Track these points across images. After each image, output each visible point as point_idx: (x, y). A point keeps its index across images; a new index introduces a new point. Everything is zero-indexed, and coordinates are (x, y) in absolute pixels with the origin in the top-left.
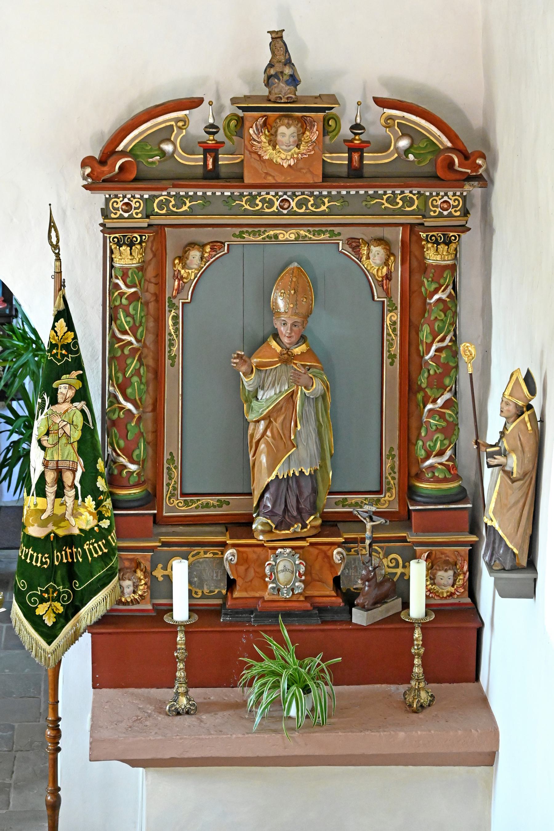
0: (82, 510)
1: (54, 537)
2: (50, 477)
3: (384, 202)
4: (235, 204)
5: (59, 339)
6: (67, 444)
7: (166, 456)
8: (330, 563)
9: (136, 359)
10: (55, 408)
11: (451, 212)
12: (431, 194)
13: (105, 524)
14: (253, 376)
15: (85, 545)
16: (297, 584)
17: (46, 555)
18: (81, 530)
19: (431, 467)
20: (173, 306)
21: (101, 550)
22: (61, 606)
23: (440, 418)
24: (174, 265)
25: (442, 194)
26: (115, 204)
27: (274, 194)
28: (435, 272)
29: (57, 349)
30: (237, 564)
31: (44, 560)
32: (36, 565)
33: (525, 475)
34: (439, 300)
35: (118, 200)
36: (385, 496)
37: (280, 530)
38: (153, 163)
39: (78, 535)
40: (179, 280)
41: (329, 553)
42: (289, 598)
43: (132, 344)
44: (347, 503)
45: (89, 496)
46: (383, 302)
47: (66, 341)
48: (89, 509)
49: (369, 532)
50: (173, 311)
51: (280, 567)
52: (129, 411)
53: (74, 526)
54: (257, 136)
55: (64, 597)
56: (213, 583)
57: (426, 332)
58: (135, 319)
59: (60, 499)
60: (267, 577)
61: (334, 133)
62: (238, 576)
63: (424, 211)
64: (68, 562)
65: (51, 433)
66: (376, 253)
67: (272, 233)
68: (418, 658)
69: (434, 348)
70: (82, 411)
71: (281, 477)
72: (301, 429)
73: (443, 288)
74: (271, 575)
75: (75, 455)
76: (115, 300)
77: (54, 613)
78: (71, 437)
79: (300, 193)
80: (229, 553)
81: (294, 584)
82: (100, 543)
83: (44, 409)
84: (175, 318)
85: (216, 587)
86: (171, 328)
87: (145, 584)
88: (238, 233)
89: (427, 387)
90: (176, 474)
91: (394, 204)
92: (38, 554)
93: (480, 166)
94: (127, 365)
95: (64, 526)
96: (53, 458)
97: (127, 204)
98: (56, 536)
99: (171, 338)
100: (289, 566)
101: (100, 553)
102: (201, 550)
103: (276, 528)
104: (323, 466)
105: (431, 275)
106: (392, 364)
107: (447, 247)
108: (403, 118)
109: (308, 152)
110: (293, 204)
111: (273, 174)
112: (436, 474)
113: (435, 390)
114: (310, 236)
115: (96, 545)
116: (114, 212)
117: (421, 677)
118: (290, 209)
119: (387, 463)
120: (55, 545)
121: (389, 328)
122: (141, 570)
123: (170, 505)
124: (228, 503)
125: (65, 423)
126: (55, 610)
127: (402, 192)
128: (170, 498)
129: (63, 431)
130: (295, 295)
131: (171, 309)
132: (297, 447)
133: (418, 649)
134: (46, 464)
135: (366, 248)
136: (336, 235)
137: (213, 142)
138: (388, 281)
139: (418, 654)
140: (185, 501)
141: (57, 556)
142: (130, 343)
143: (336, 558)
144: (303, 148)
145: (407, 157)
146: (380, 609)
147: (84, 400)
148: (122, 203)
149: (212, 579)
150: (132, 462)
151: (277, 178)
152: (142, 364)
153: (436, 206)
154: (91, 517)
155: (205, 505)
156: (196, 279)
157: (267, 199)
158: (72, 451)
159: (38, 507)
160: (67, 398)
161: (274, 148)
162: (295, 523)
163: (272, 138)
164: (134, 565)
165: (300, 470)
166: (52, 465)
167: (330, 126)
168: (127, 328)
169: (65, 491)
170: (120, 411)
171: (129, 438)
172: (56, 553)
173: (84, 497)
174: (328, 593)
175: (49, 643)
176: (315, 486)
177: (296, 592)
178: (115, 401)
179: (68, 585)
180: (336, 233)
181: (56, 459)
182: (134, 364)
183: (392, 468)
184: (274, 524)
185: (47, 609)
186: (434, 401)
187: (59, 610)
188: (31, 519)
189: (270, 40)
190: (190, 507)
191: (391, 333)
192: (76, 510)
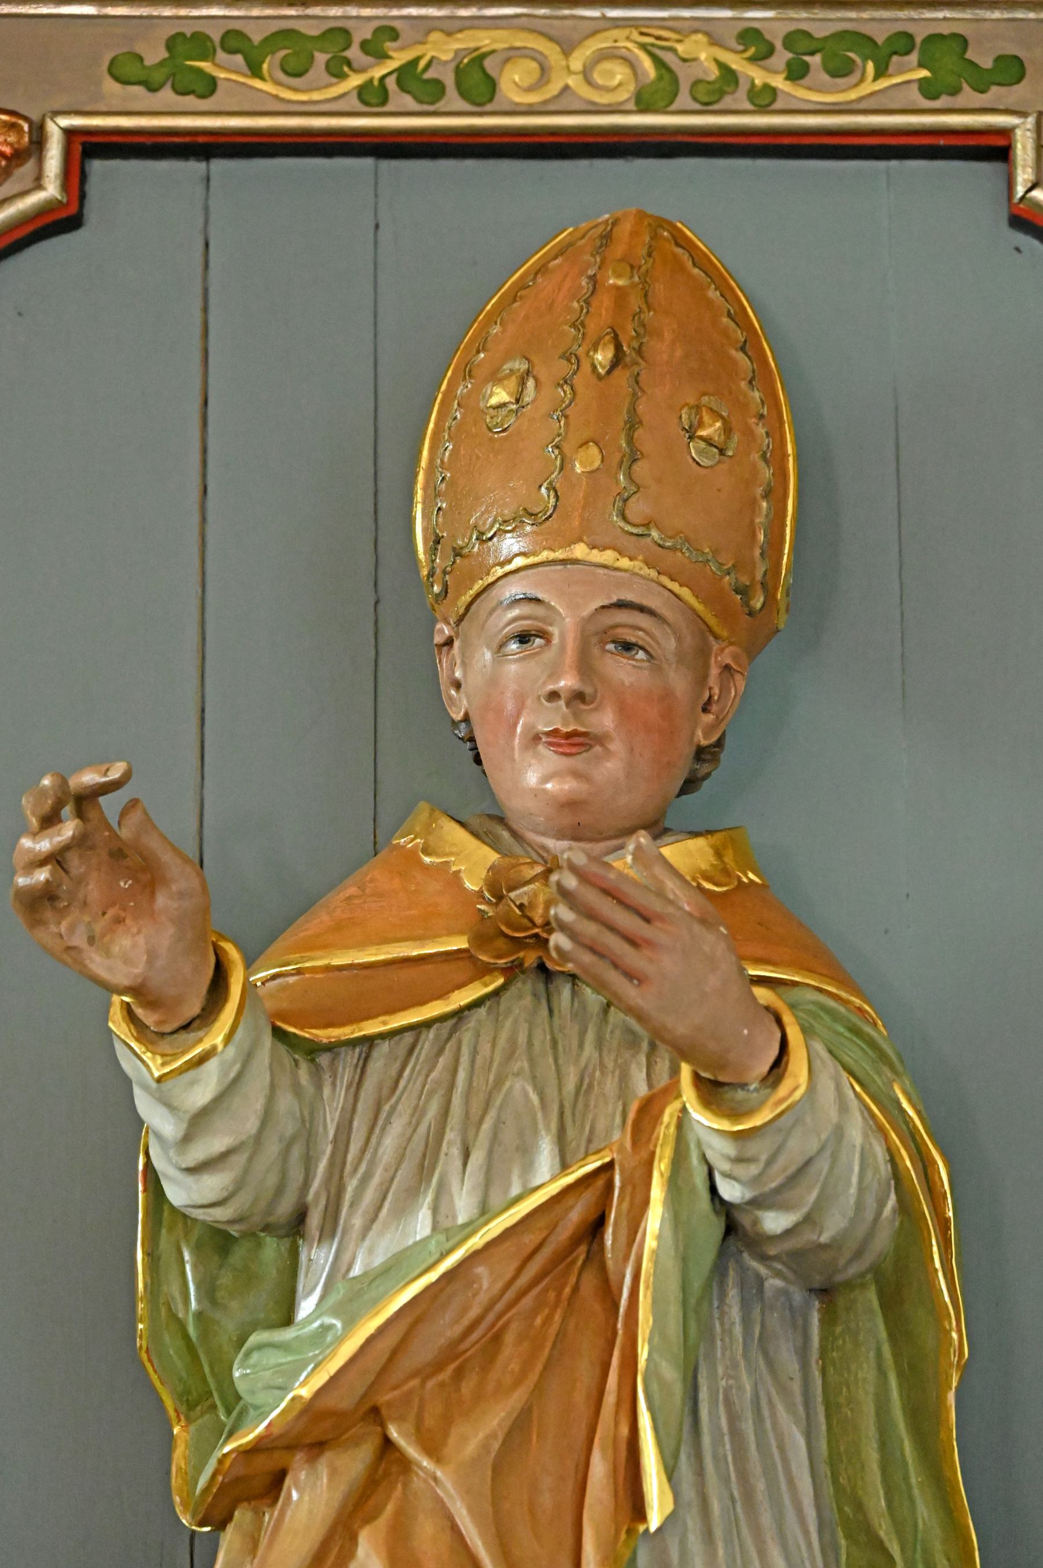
14: (216, 1036)
72: (670, 1520)
114: (759, 76)
130: (622, 377)
136: (982, 82)
180: (987, 63)
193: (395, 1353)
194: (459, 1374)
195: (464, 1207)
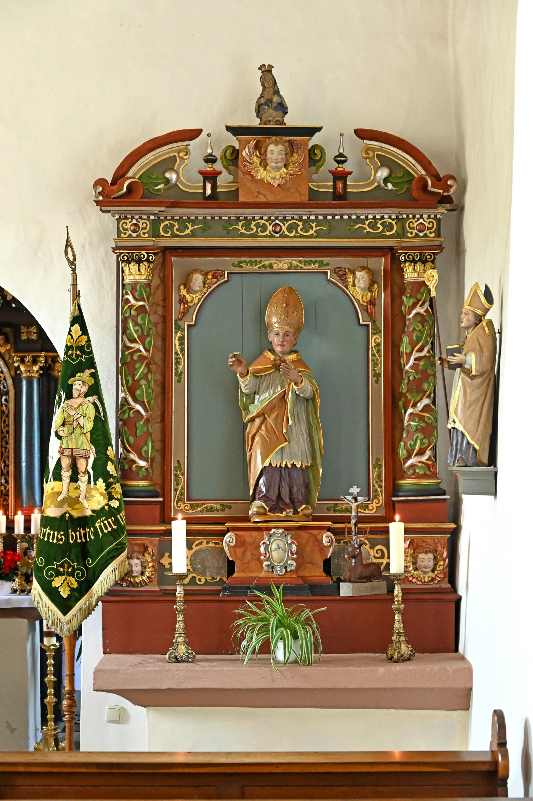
0: (94, 493)
1: (69, 517)
2: (66, 463)
3: (366, 226)
4: (232, 228)
5: (75, 341)
6: (81, 434)
8: (320, 546)
9: (144, 364)
10: (70, 402)
11: (426, 233)
12: (408, 216)
13: (115, 504)
14: (248, 377)
15: (97, 523)
16: (289, 562)
17: (62, 533)
18: (93, 511)
19: (412, 466)
20: (178, 328)
21: (111, 526)
23: (420, 419)
24: (179, 290)
25: (418, 216)
26: (124, 225)
27: (267, 219)
28: (413, 288)
29: (73, 350)
30: (234, 547)
31: (59, 537)
32: (53, 542)
33: (482, 374)
34: (417, 314)
36: (372, 503)
37: (274, 513)
38: (159, 190)
39: (91, 516)
40: (184, 304)
41: (319, 537)
42: (282, 575)
43: (141, 351)
44: (338, 508)
45: (100, 478)
46: (368, 325)
47: (81, 343)
48: (100, 490)
49: (355, 512)
50: (179, 332)
51: (274, 546)
52: (138, 411)
54: (250, 158)
55: (78, 574)
56: (215, 570)
57: (406, 343)
58: (143, 328)
59: (74, 483)
60: (261, 555)
61: (320, 163)
62: (237, 558)
63: (402, 235)
64: (82, 542)
65: (67, 424)
66: (361, 277)
67: (267, 263)
68: (398, 613)
69: (412, 358)
70: (95, 404)
71: (274, 465)
73: (420, 303)
74: (266, 553)
75: (88, 443)
76: (126, 312)
77: (69, 586)
79: (290, 218)
80: (229, 537)
81: (287, 562)
82: (110, 520)
83: (60, 403)
85: (218, 574)
86: (177, 347)
87: (153, 567)
88: (236, 263)
89: (407, 392)
90: (184, 480)
91: (376, 228)
92: (54, 532)
93: (451, 186)
94: (136, 369)
95: (78, 508)
96: (69, 447)
97: (135, 225)
98: (71, 516)
99: (178, 357)
100: (281, 544)
101: (110, 529)
102: (204, 540)
103: (269, 511)
104: (314, 466)
105: (410, 291)
106: (377, 382)
107: (423, 265)
108: (381, 149)
109: (295, 172)
110: (284, 228)
111: (264, 193)
112: (417, 471)
113: (415, 394)
114: (301, 265)
115: (106, 522)
116: (124, 232)
117: (401, 631)
118: (281, 233)
119: (373, 472)
120: (69, 525)
121: (374, 349)
122: (149, 554)
123: (179, 509)
125: (79, 416)
126: (70, 585)
127: (382, 218)
128: (177, 504)
129: (78, 423)
131: (177, 331)
132: (289, 443)
133: (398, 604)
134: (62, 452)
135: (352, 277)
136: (325, 265)
137: (211, 169)
138: (372, 306)
139: (399, 610)
140: (191, 504)
141: (72, 535)
142: (139, 351)
143: (325, 540)
144: (291, 168)
145: (386, 186)
146: (366, 585)
147: (96, 395)
148: (131, 224)
149: (214, 566)
150: (141, 457)
151: (267, 197)
152: (149, 371)
153: (413, 228)
154: (102, 497)
155: (209, 509)
156: (200, 303)
157: (261, 224)
158: (86, 440)
159: (55, 490)
160: (81, 393)
161: (265, 169)
162: (289, 508)
163: (263, 157)
164: (142, 549)
165: (292, 463)
166: (66, 452)
167: (316, 155)
168: (136, 336)
169: (79, 476)
170: (130, 411)
171: (138, 435)
172: (71, 532)
173: (96, 480)
174: (318, 574)
175: (65, 614)
176: (307, 481)
177: (288, 570)
178: (126, 404)
179: (81, 561)
181: (71, 447)
182: (142, 370)
183: (379, 477)
184: (268, 507)
185: (62, 582)
186: (415, 405)
187: (73, 585)
188: (48, 501)
189: (261, 74)
191: (376, 353)
192: (89, 493)
193: (266, 408)
194: (271, 410)
195: (272, 392)
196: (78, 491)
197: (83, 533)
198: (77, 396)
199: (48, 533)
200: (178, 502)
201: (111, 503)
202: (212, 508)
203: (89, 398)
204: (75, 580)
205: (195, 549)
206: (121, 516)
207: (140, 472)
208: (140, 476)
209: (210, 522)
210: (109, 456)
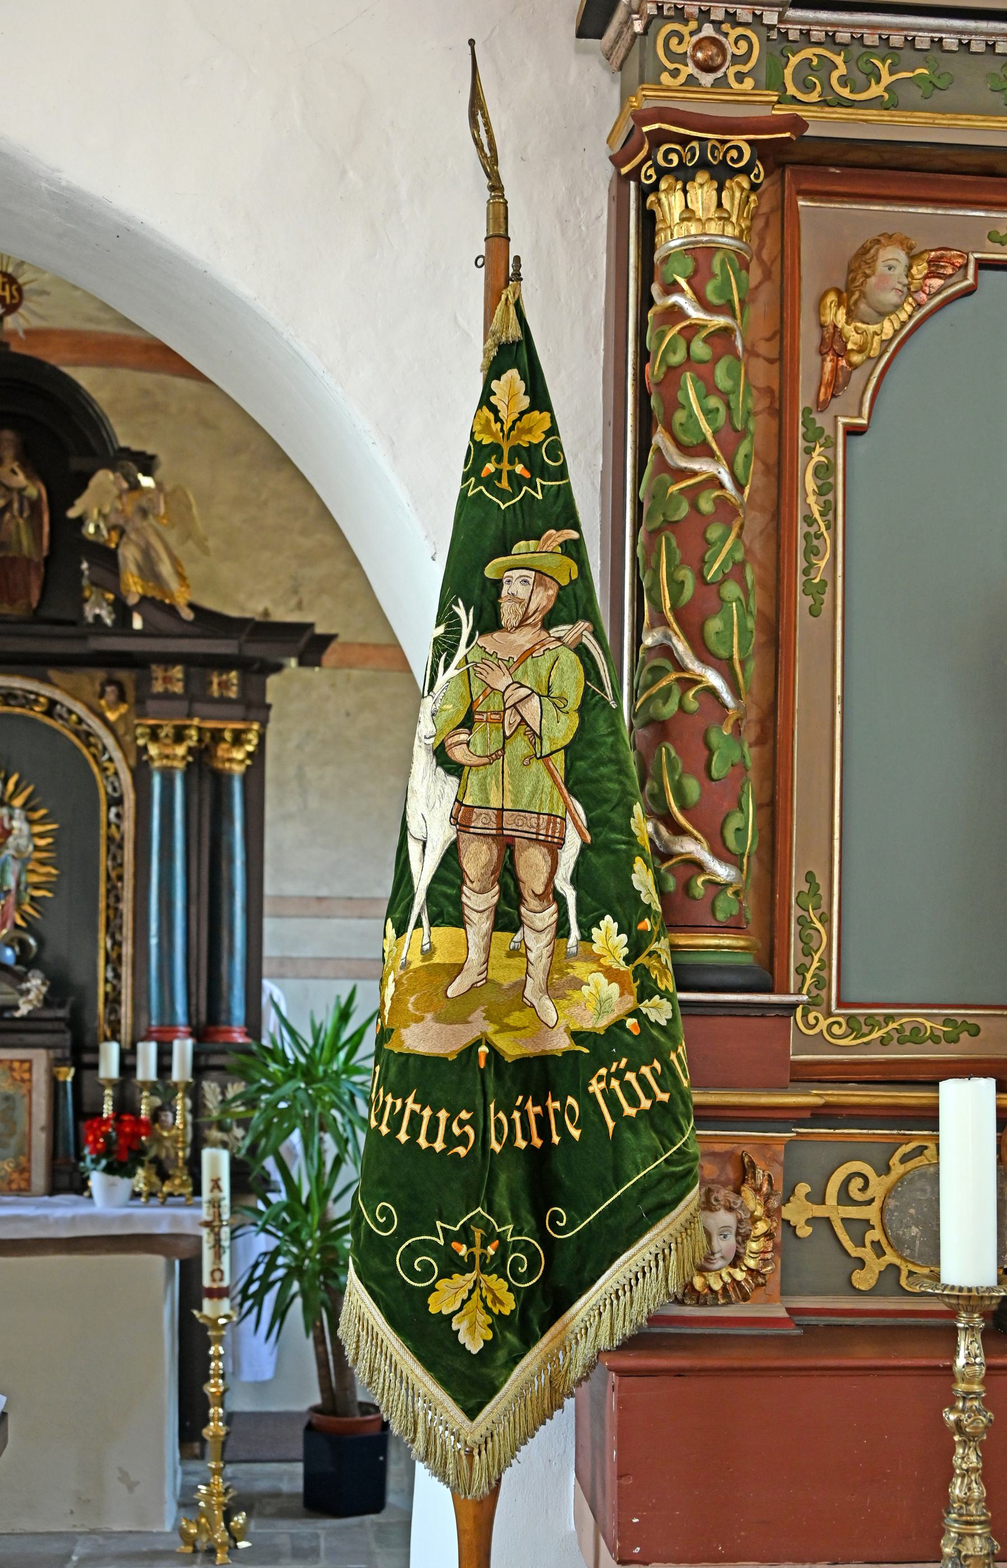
0: (580, 969)
1: (488, 1056)
7: (797, 885)
15: (594, 1081)
17: (464, 1115)
18: (577, 1036)
20: (815, 435)
21: (649, 1093)
22: (509, 1290)
26: (674, 41)
29: (499, 461)
31: (456, 1130)
32: (431, 1149)
35: (685, 30)
39: (567, 1054)
47: (527, 438)
50: (818, 450)
52: (711, 692)
53: (551, 1024)
58: (732, 405)
59: (506, 935)
64: (530, 1147)
65: (481, 721)
70: (581, 651)
75: (556, 793)
78: (545, 738)
82: (645, 1070)
83: (455, 647)
84: (823, 470)
86: (811, 499)
87: (768, 1235)
92: (436, 1110)
94: (709, 544)
95: (519, 1024)
96: (488, 802)
98: (495, 1054)
101: (646, 1104)
116: (671, 66)
122: (757, 1190)
123: (811, 1032)
124: (975, 1031)
125: (524, 692)
129: (519, 719)
140: (850, 1018)
142: (715, 482)
147: (586, 618)
148: (695, 39)
154: (615, 987)
155: (907, 1033)
158: (548, 782)
159: (437, 959)
160: (531, 610)
168: (707, 430)
169: (523, 910)
170: (689, 689)
171: (715, 774)
172: (496, 1113)
179: (529, 1222)
181: (495, 802)
185: (465, 1296)
187: (502, 1303)
188: (412, 999)
190: (865, 1040)
192: (560, 971)
196: (519, 962)
197: (537, 1116)
198: (515, 622)
199: (413, 1112)
200: (809, 1012)
201: (645, 1007)
202: (916, 1030)
203: (561, 630)
204: (506, 1285)
205: (898, 1169)
206: (678, 1057)
207: (720, 904)
208: (721, 916)
209: (921, 1077)
210: (636, 837)
